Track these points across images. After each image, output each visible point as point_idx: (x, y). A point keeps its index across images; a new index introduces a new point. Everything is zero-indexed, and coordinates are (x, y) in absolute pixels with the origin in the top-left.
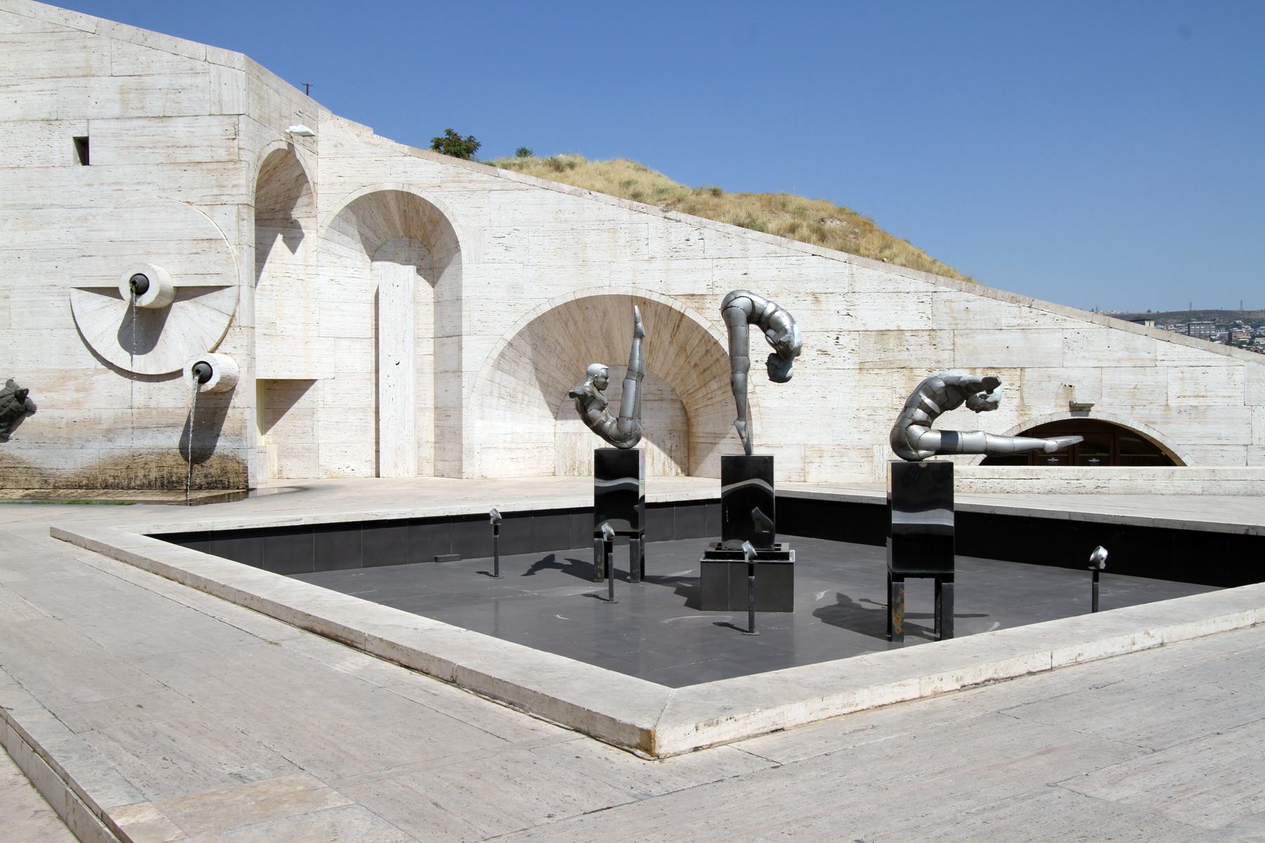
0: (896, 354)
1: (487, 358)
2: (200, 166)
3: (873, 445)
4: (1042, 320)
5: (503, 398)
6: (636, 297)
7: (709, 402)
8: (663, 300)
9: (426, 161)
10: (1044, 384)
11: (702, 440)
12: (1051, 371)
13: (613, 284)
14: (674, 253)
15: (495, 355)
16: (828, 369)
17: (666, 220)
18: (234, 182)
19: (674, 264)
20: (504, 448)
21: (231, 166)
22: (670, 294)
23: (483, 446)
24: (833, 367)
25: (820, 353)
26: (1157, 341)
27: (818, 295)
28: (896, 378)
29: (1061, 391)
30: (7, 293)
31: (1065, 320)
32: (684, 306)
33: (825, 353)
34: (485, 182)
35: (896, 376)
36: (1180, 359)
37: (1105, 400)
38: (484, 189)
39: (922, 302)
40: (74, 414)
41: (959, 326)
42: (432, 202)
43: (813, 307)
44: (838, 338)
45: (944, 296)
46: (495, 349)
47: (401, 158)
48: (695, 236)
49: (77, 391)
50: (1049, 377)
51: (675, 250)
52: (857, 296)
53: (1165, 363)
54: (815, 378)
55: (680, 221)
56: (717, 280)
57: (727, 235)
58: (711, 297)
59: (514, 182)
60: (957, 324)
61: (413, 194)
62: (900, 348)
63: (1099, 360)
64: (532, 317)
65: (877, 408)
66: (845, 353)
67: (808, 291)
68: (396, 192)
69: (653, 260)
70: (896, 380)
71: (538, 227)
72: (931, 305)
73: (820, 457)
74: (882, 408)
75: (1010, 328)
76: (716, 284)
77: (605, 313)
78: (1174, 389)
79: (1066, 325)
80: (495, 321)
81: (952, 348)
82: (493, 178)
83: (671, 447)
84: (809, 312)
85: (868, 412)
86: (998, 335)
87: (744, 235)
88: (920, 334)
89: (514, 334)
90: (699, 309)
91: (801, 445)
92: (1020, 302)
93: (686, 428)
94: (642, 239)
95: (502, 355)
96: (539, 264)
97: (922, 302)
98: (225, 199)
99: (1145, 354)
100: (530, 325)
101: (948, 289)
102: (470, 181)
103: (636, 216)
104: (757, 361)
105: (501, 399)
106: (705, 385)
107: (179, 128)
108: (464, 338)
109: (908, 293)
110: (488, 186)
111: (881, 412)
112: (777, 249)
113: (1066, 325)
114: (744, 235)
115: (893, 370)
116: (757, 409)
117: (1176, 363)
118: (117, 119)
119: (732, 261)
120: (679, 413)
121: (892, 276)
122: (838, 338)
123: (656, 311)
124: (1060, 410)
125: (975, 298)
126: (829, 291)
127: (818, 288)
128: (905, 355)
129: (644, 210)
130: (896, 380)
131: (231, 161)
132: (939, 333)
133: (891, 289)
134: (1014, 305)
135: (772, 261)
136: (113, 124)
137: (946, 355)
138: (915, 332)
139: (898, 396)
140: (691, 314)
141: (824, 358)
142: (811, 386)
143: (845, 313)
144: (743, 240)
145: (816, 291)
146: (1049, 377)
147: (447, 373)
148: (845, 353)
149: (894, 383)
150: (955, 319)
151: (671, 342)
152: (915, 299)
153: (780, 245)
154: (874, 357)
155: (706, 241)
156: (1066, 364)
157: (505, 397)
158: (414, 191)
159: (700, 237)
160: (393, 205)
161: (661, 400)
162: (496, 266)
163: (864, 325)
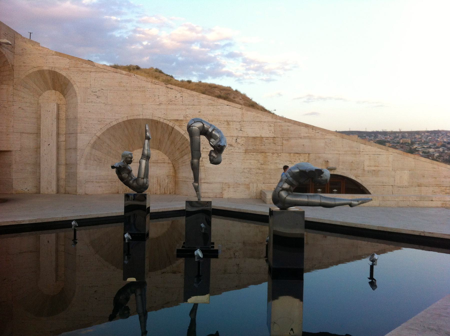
0: (260, 147)
3: (250, 183)
4: (317, 134)
5: (96, 161)
6: (154, 120)
7: (184, 164)
8: (165, 121)
9: (62, 58)
12: (320, 155)
14: (170, 102)
15: (92, 142)
16: (232, 152)
17: (167, 88)
19: (170, 107)
20: (96, 182)
22: (168, 119)
23: (86, 181)
24: (235, 151)
25: (229, 145)
26: (361, 144)
27: (229, 122)
28: (260, 156)
29: (324, 163)
31: (326, 135)
32: (174, 124)
34: (88, 68)
35: (259, 156)
36: (369, 152)
37: (341, 167)
38: (88, 71)
39: (271, 126)
41: (285, 136)
42: (64, 75)
44: (236, 140)
45: (279, 124)
46: (92, 140)
47: (51, 56)
51: (170, 101)
52: (244, 123)
53: (363, 153)
54: (227, 155)
55: (172, 89)
56: (188, 114)
57: (192, 96)
58: (185, 121)
59: (101, 68)
61: (56, 72)
62: (262, 144)
63: (338, 151)
64: (108, 126)
65: (252, 168)
67: (225, 120)
68: (49, 70)
69: (161, 105)
70: (259, 157)
71: (111, 89)
72: (274, 127)
73: (229, 188)
74: (254, 168)
75: (305, 137)
76: (187, 116)
79: (326, 137)
80: (92, 128)
81: (282, 145)
82: (92, 66)
83: (168, 182)
84: (225, 128)
85: (248, 170)
87: (199, 96)
88: (269, 139)
89: (100, 133)
90: (180, 126)
91: (221, 183)
92: (309, 127)
93: (174, 175)
94: (156, 96)
95: (95, 142)
96: (112, 104)
97: (271, 126)
99: (356, 149)
100: (108, 130)
101: (281, 121)
102: (82, 67)
103: (154, 86)
104: (204, 148)
106: (182, 157)
108: (78, 135)
109: (265, 122)
110: (90, 70)
111: (253, 170)
112: (213, 102)
113: (326, 137)
114: (199, 96)
115: (259, 153)
116: (203, 167)
117: (367, 153)
119: (194, 107)
120: (172, 168)
121: (259, 115)
122: (236, 140)
125: (291, 125)
126: (233, 120)
127: (229, 119)
128: (263, 147)
129: (158, 83)
130: (259, 157)
132: (277, 139)
133: (258, 120)
134: (306, 128)
135: (210, 107)
137: (279, 148)
138: (267, 138)
139: (260, 164)
140: (177, 128)
141: (231, 148)
142: (225, 159)
143: (240, 129)
144: (199, 98)
145: (228, 120)
146: (319, 157)
147: (71, 150)
148: (239, 146)
149: (259, 158)
150: (283, 133)
151: (168, 139)
152: (268, 125)
153: (214, 101)
154: (251, 148)
156: (326, 152)
157: (97, 160)
158: (57, 70)
159: (181, 96)
160: (48, 76)
161: (164, 163)
162: (93, 104)
163: (247, 134)
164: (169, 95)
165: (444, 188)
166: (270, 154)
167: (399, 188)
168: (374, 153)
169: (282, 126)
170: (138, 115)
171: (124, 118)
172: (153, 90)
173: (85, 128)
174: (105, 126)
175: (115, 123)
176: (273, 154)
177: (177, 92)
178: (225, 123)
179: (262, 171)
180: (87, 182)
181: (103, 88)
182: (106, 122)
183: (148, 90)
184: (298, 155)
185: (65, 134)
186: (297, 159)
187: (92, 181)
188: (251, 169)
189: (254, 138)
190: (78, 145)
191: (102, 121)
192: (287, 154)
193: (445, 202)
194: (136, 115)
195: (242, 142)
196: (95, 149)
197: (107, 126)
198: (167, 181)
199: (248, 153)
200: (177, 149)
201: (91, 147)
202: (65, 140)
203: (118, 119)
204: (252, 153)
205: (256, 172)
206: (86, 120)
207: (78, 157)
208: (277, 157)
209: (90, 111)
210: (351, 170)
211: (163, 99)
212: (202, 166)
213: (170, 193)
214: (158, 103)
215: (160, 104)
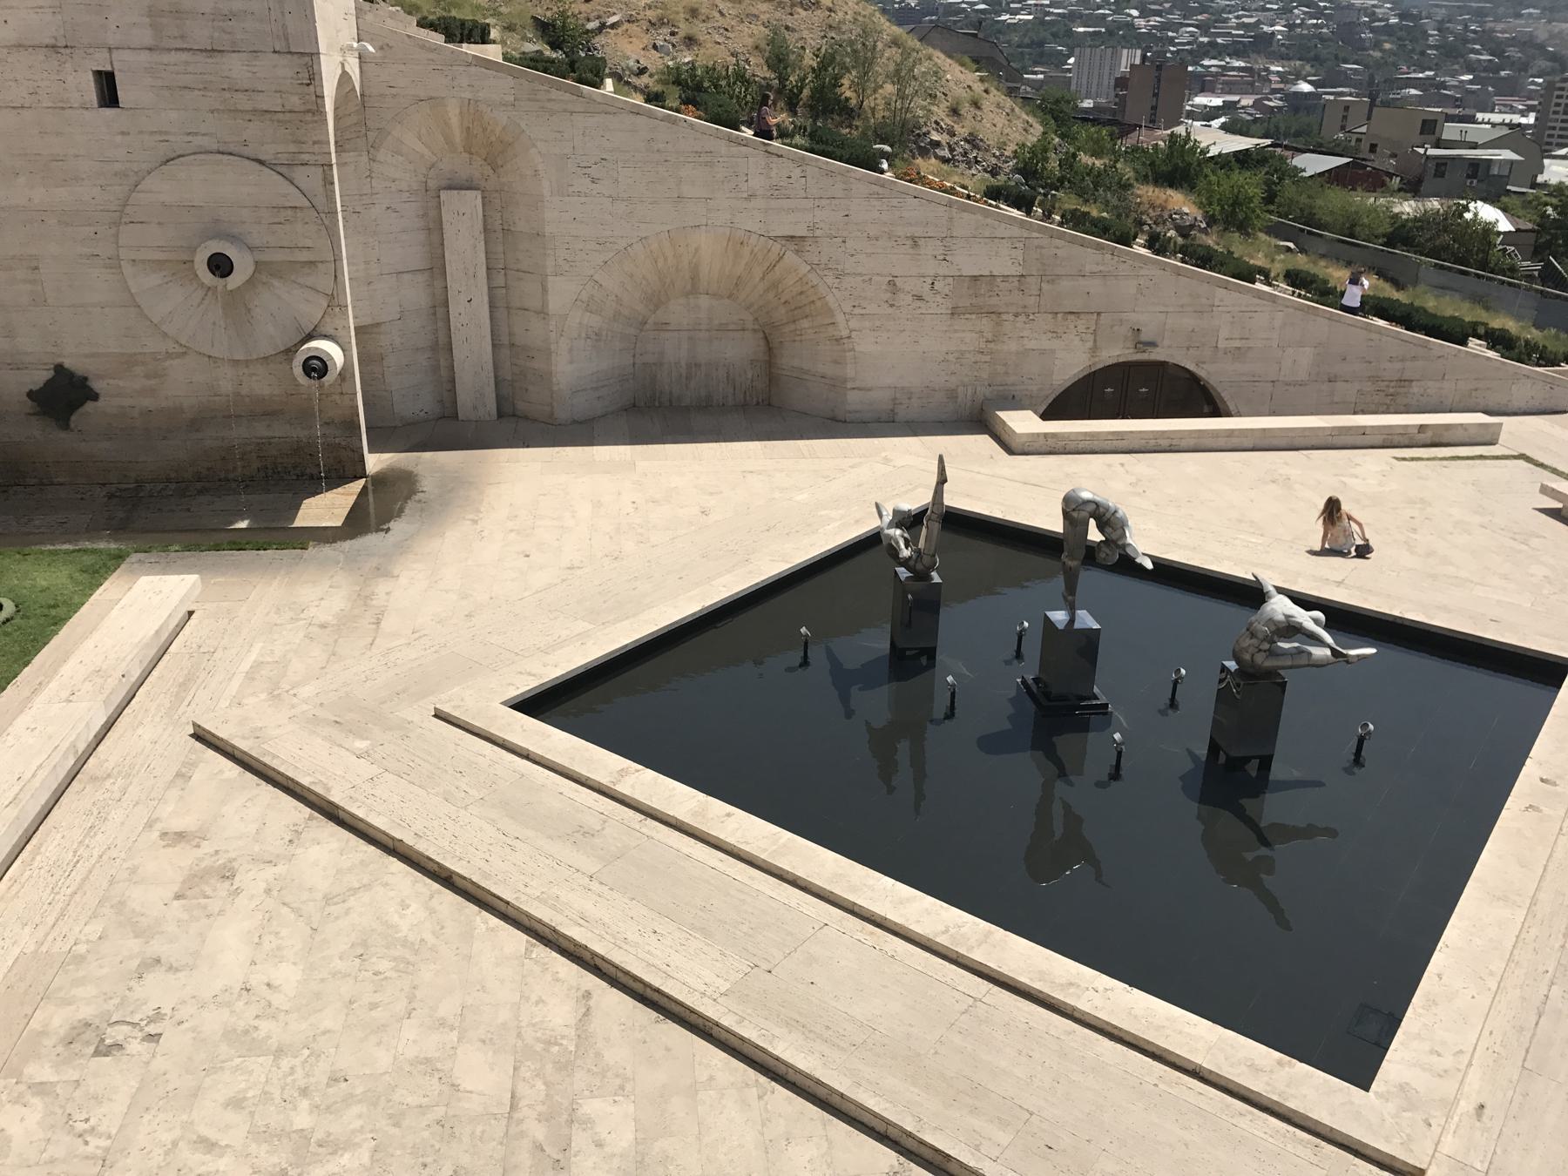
2: (268, 116)
4: (1122, 267)
7: (798, 338)
9: (495, 73)
10: (1115, 328)
11: (784, 373)
13: (710, 222)
14: (775, 192)
18: (315, 139)
19: (774, 203)
21: (309, 117)
27: (916, 239)
30: (34, 264)
33: (920, 298)
35: (985, 321)
40: (147, 402)
43: (911, 251)
45: (1036, 242)
48: (797, 172)
49: (147, 377)
50: (1121, 320)
54: (909, 323)
55: (782, 156)
57: (830, 174)
60: (1045, 270)
66: (939, 298)
74: (969, 352)
77: (697, 250)
78: (1224, 333)
79: (1142, 272)
85: (956, 355)
86: (1082, 281)
88: (1011, 279)
93: (767, 358)
98: (305, 157)
107: (236, 67)
111: (967, 355)
112: (881, 190)
113: (1142, 272)
118: (150, 49)
119: (834, 201)
120: (762, 343)
123: (752, 251)
124: (1127, 352)
126: (929, 235)
127: (918, 232)
128: (994, 301)
131: (309, 111)
132: (1028, 279)
133: (987, 235)
135: (875, 203)
136: (144, 57)
137: (1032, 301)
138: (1005, 278)
141: (919, 303)
143: (942, 257)
145: (916, 235)
148: (939, 298)
151: (763, 279)
155: (809, 179)
161: (743, 330)
162: (583, 199)
163: (959, 270)
164: (773, 174)
165: (1386, 383)
166: (1011, 317)
167: (1287, 387)
168: (1244, 309)
169: (1042, 247)
172: (734, 159)
176: (1016, 315)
177: (791, 164)
178: (907, 242)
179: (987, 358)
181: (607, 158)
183: (720, 159)
184: (1072, 317)
186: (1072, 326)
188: (962, 353)
189: (975, 278)
190: (551, 306)
192: (1050, 316)
193: (1390, 437)
195: (946, 291)
196: (591, 312)
198: (750, 376)
199: (959, 315)
200: (783, 300)
204: (967, 316)
205: (973, 360)
207: (553, 335)
208: (1025, 323)
210: (1188, 349)
211: (757, 183)
212: (850, 351)
213: (758, 403)
214: (745, 195)
215: (751, 196)
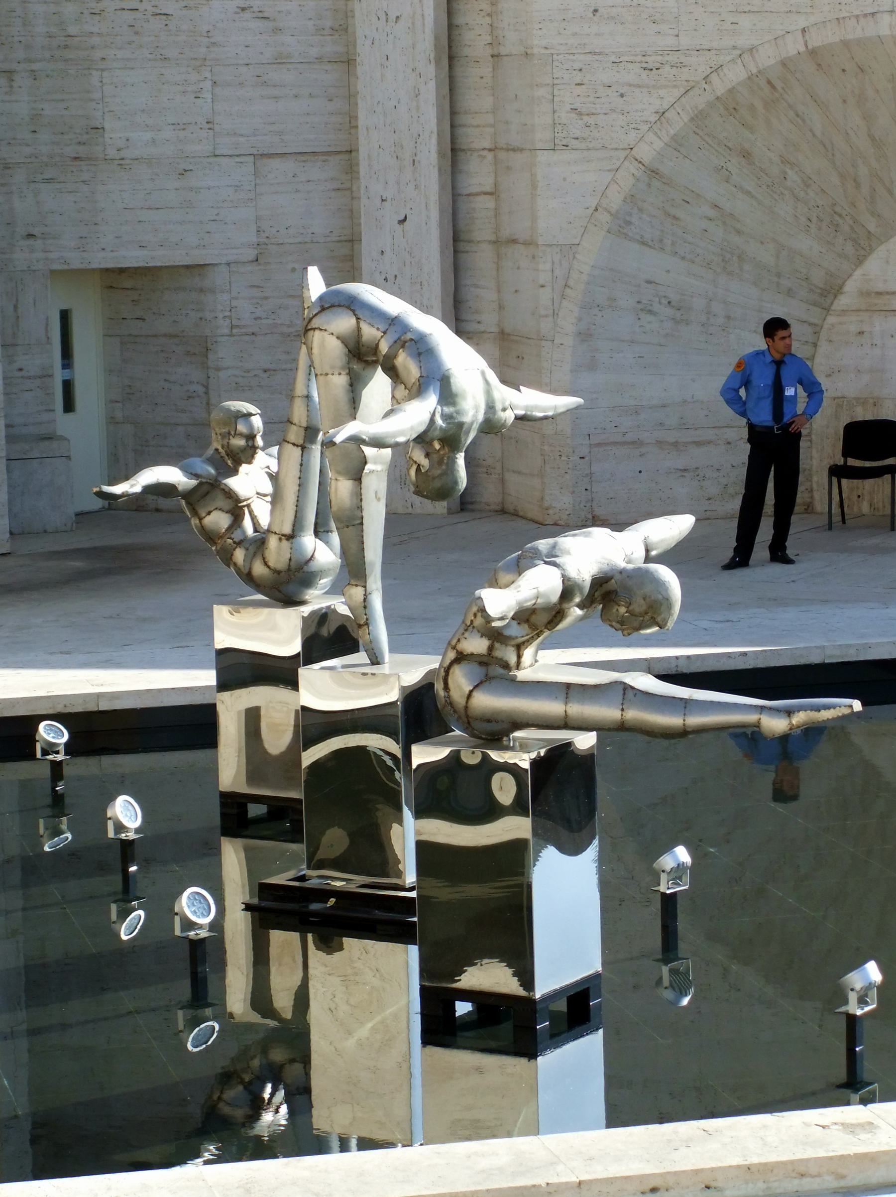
1: (596, 210)
5: (650, 312)
15: (615, 200)
20: (659, 443)
23: (595, 440)
80: (613, 110)
89: (658, 144)
100: (699, 118)
105: (643, 315)
157: (656, 307)
170: (865, 16)
171: (789, 38)
173: (573, 115)
174: (683, 99)
175: (735, 74)
180: (599, 445)
182: (686, 70)
185: (490, 150)
187: (629, 437)
191: (667, 68)
194: (857, 17)
197: (691, 93)
201: (608, 231)
202: (496, 185)
203: (752, 50)
206: (577, 66)
209: (596, 11)
